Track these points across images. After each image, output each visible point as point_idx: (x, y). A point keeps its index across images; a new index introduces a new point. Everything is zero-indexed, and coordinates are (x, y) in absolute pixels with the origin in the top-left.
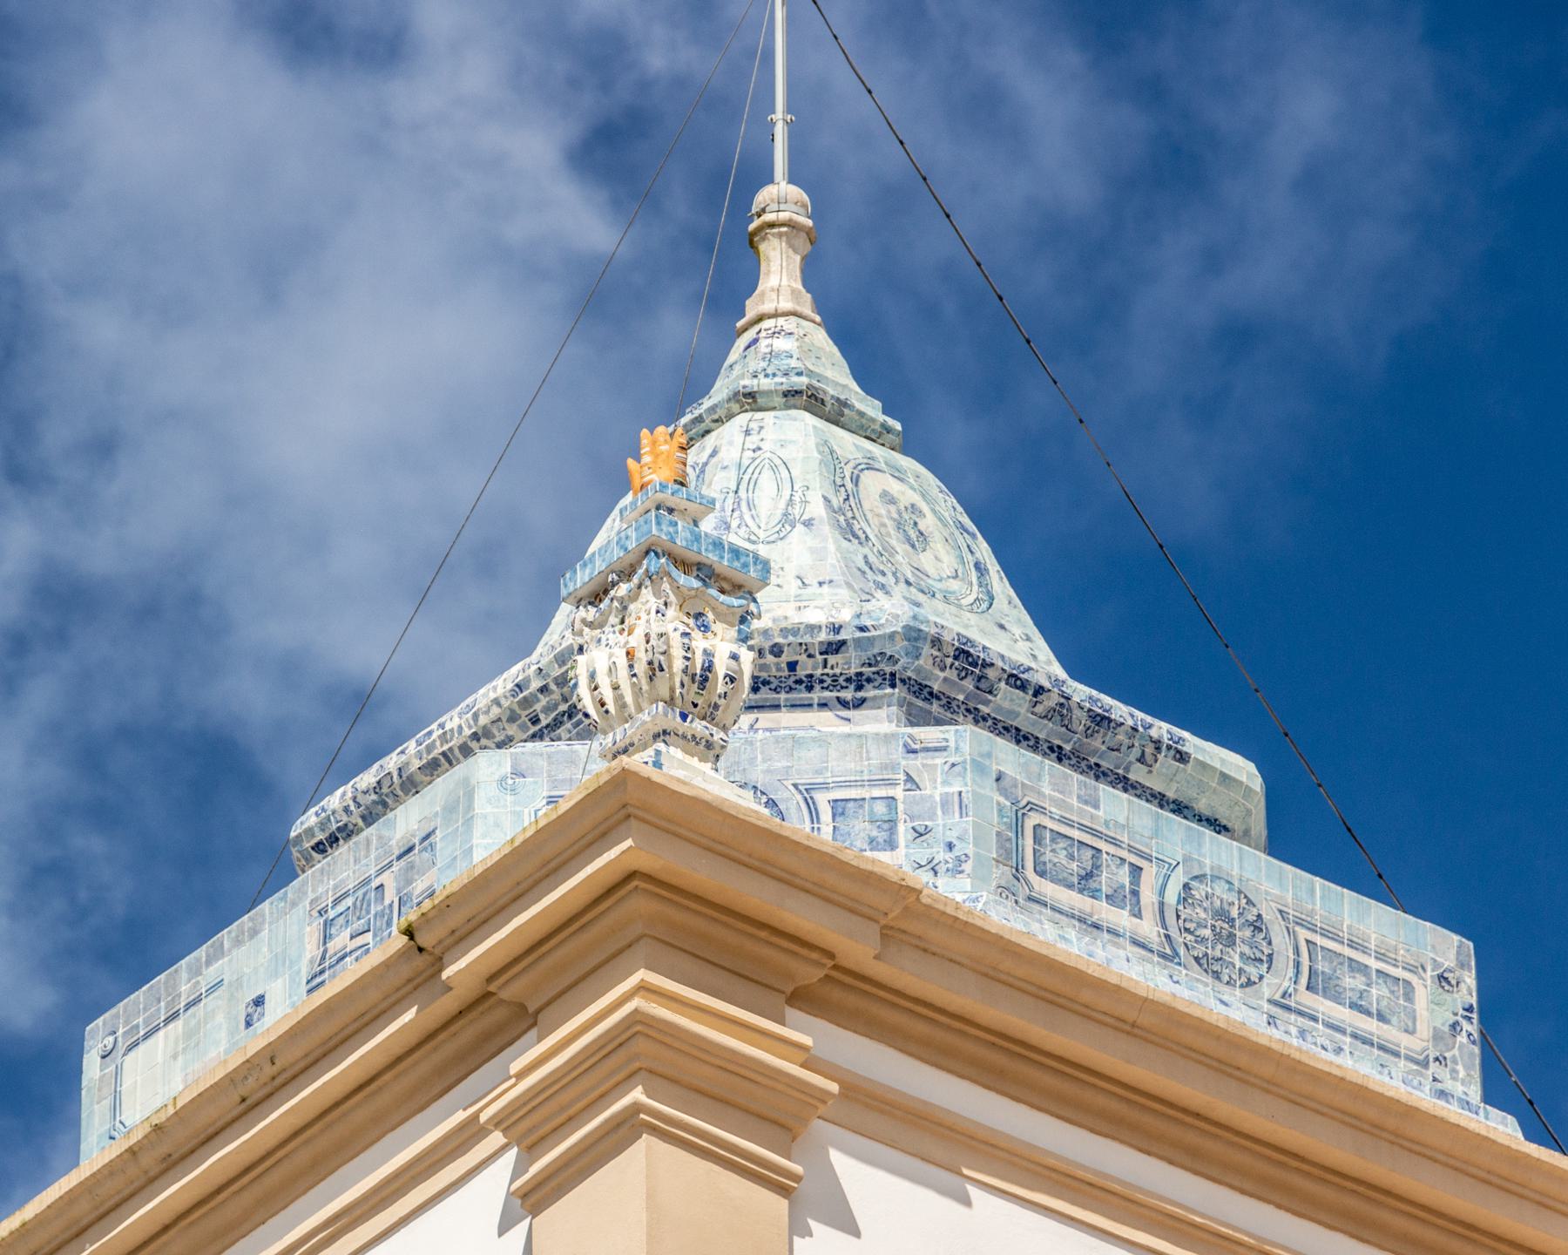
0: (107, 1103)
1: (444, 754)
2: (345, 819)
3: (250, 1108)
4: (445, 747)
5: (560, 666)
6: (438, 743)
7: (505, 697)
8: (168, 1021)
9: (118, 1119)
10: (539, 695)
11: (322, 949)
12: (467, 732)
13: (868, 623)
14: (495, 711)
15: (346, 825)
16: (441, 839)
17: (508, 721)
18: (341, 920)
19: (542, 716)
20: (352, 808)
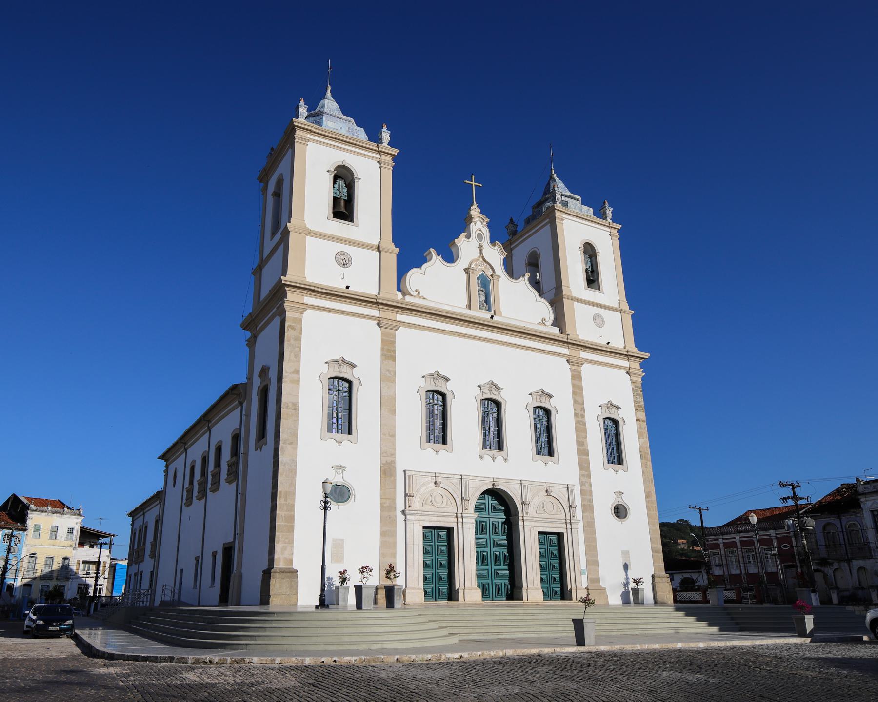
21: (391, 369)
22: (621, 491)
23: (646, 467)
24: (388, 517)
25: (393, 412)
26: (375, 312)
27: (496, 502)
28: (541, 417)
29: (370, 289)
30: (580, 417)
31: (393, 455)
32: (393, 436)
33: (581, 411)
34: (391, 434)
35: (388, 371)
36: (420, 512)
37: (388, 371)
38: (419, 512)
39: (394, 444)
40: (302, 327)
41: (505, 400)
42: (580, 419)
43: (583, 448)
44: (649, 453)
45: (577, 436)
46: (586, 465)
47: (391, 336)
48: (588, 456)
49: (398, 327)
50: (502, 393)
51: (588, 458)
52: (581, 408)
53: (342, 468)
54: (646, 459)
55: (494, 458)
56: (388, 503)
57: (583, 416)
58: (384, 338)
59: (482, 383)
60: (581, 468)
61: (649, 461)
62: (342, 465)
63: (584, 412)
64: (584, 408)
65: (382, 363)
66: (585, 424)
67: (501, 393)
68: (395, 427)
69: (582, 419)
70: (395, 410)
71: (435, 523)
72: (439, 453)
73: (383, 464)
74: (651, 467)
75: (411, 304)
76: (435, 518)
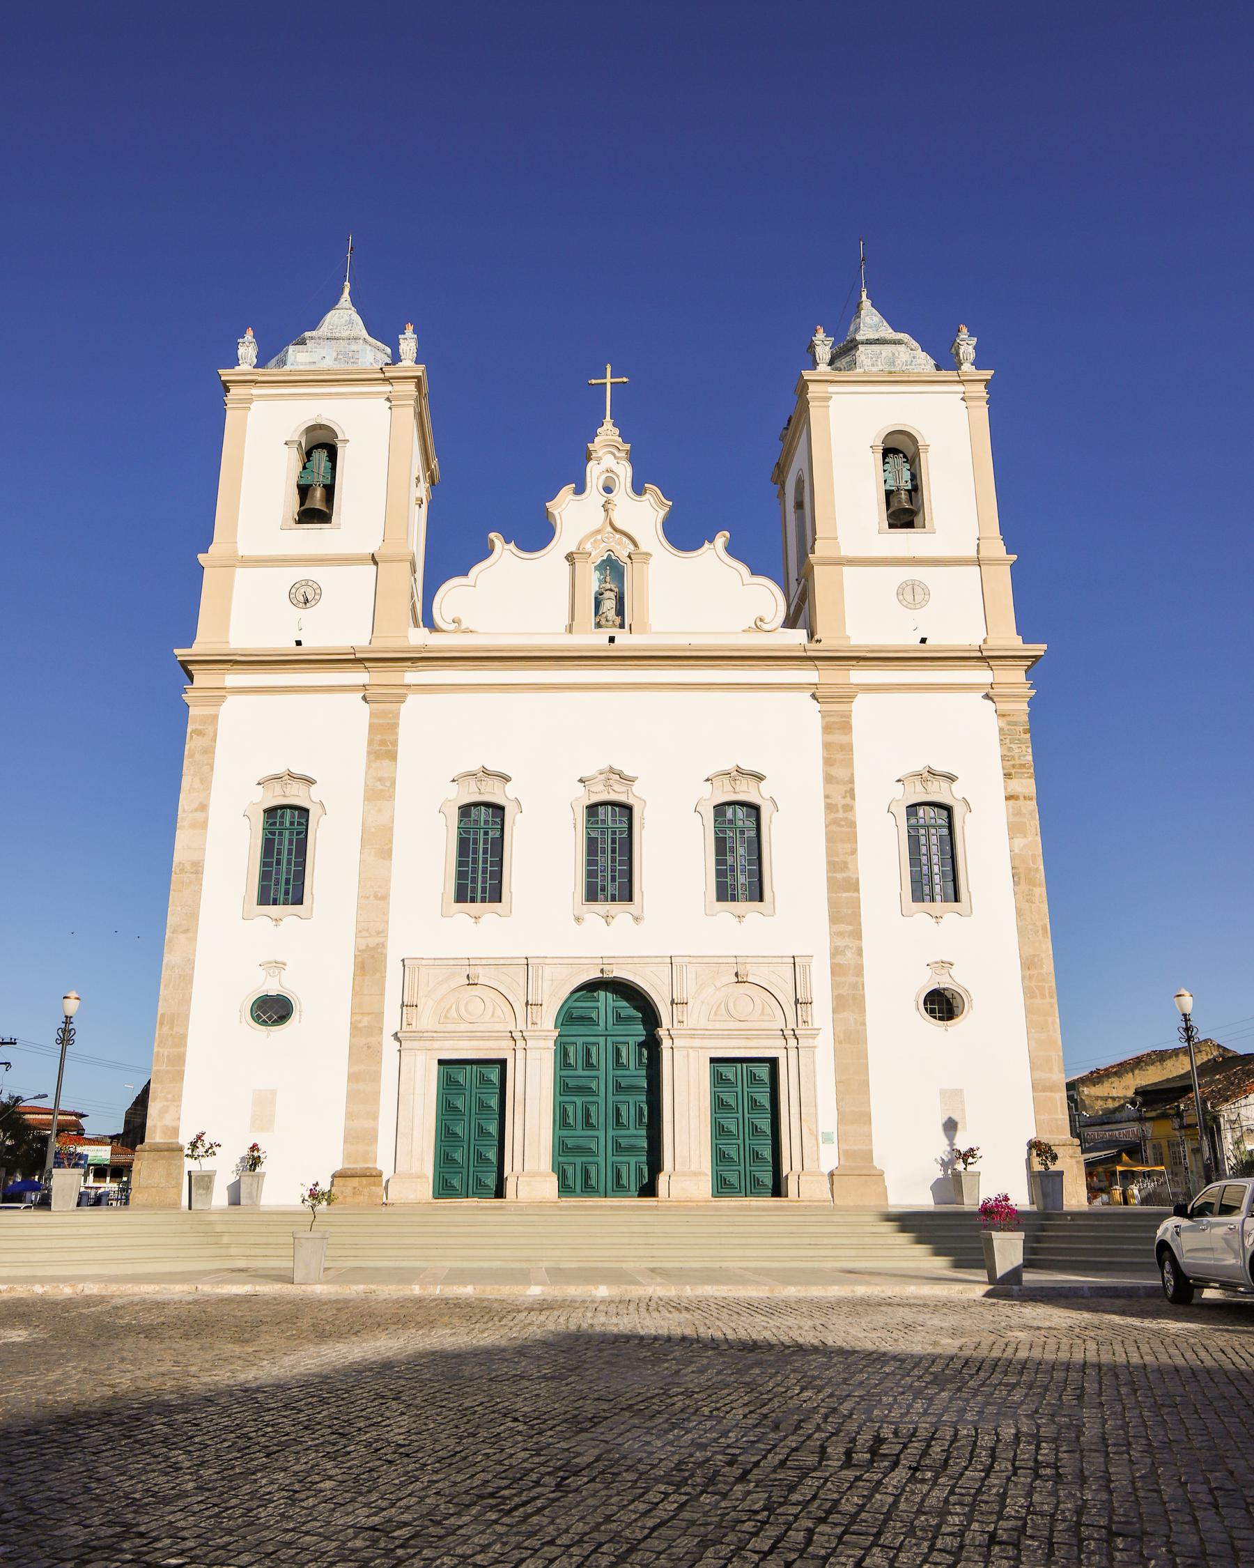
21: (386, 775)
22: (945, 960)
23: (1030, 901)
24: (365, 1048)
25: (386, 853)
26: (359, 677)
27: (625, 1004)
28: (740, 823)
29: (357, 638)
30: (841, 810)
31: (382, 933)
32: (384, 898)
33: (844, 797)
34: (379, 895)
35: (380, 779)
36: (429, 1034)
37: (380, 779)
38: (425, 1034)
39: (385, 913)
41: (644, 800)
42: (841, 815)
43: (844, 875)
44: (1042, 867)
45: (830, 851)
46: (850, 912)
48: (857, 890)
49: (405, 696)
50: (636, 787)
51: (855, 895)
52: (846, 792)
53: (279, 965)
54: (1031, 882)
55: (607, 918)
56: (365, 1021)
57: (849, 808)
58: (376, 721)
59: (585, 774)
60: (834, 918)
61: (1040, 885)
62: (278, 959)
63: (853, 798)
64: (852, 790)
65: (368, 767)
66: (852, 824)
67: (634, 788)
68: (388, 880)
69: (845, 815)
70: (390, 850)
71: (465, 1051)
72: (480, 920)
73: (359, 951)
74: (1045, 899)
76: (466, 1044)
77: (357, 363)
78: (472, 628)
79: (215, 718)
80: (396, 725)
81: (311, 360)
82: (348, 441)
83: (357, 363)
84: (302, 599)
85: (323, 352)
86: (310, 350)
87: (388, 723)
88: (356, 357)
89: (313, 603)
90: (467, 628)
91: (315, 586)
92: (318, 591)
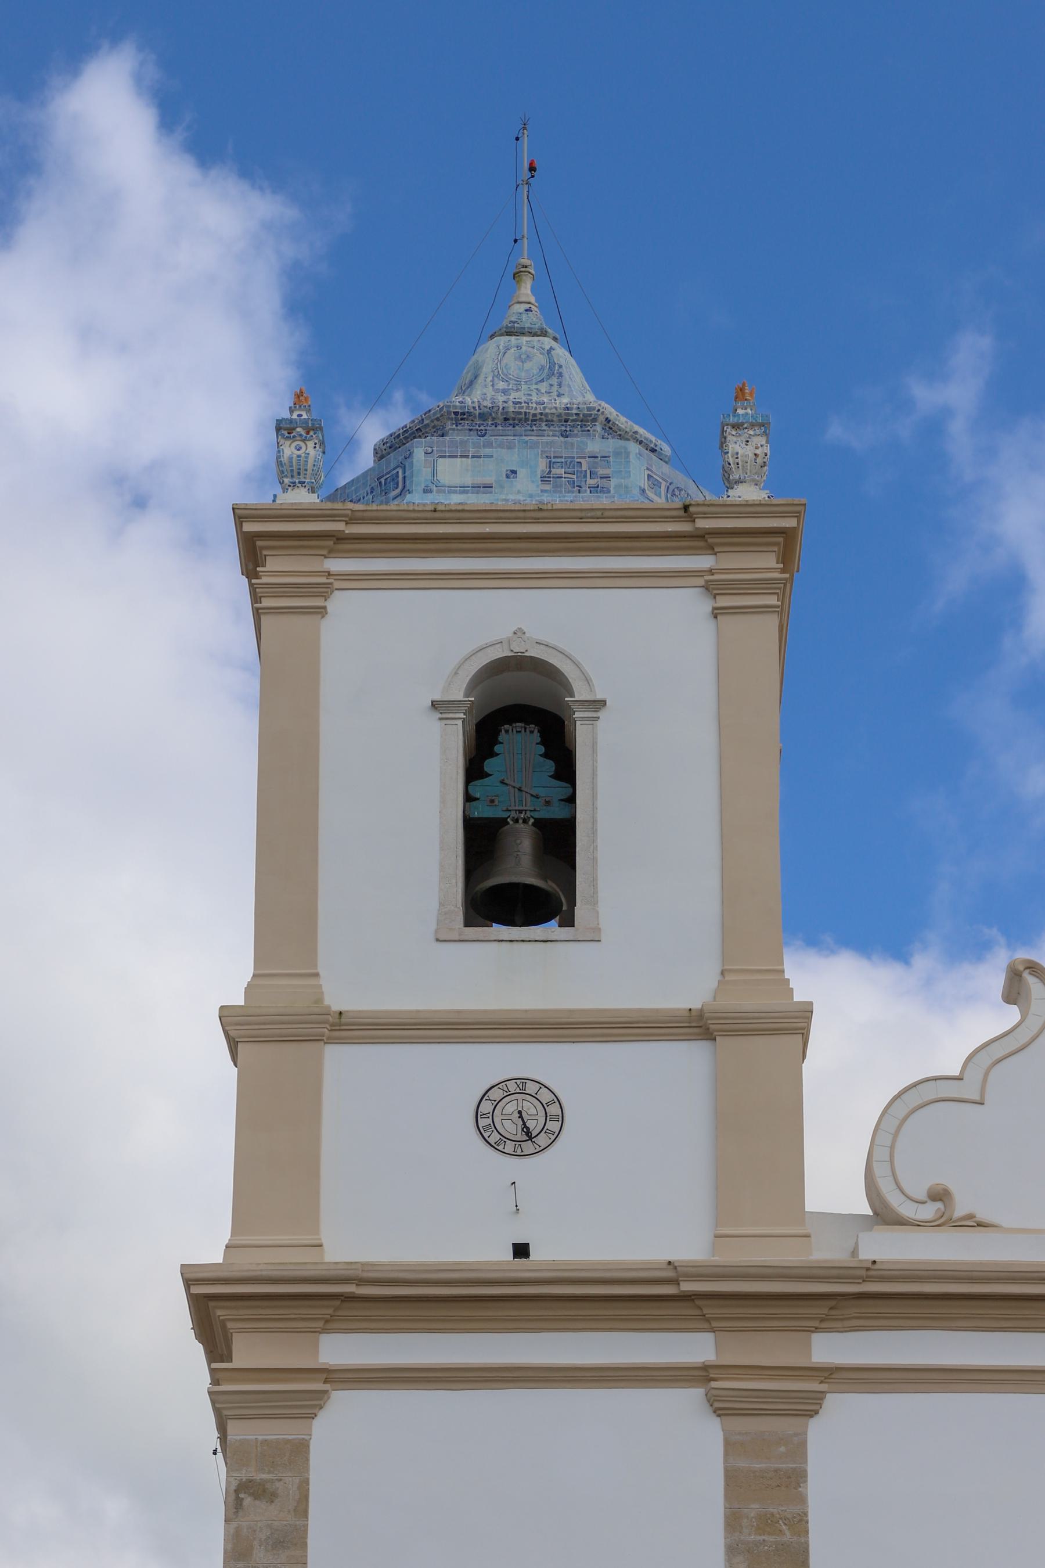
0: (429, 470)
1: (525, 413)
2: (472, 410)
3: (581, 520)
4: (527, 411)
5: (587, 411)
6: (525, 408)
7: (561, 409)
8: (462, 457)
9: (435, 478)
10: (574, 415)
11: (548, 470)
12: (539, 411)
13: (663, 449)
14: (554, 411)
15: (471, 412)
16: (613, 461)
17: (557, 416)
18: (559, 464)
19: (569, 421)
20: (477, 408)
40: (307, 1482)
47: (782, 1449)
58: (742, 1463)
75: (871, 1270)
77: (606, 490)
78: (982, 1216)
79: (300, 1450)
80: (796, 1478)
81: (480, 480)
82: (603, 703)
83: (606, 490)
84: (511, 1128)
85: (511, 458)
86: (472, 451)
87: (776, 1471)
88: (601, 472)
89: (542, 1140)
90: (971, 1217)
91: (545, 1096)
92: (554, 1110)
